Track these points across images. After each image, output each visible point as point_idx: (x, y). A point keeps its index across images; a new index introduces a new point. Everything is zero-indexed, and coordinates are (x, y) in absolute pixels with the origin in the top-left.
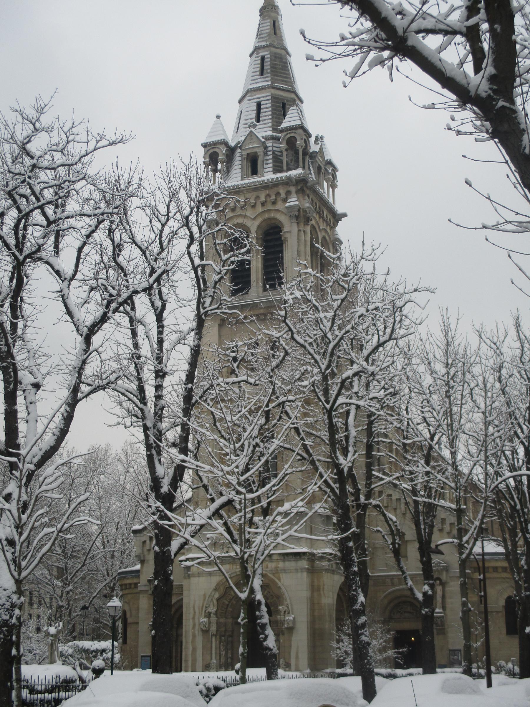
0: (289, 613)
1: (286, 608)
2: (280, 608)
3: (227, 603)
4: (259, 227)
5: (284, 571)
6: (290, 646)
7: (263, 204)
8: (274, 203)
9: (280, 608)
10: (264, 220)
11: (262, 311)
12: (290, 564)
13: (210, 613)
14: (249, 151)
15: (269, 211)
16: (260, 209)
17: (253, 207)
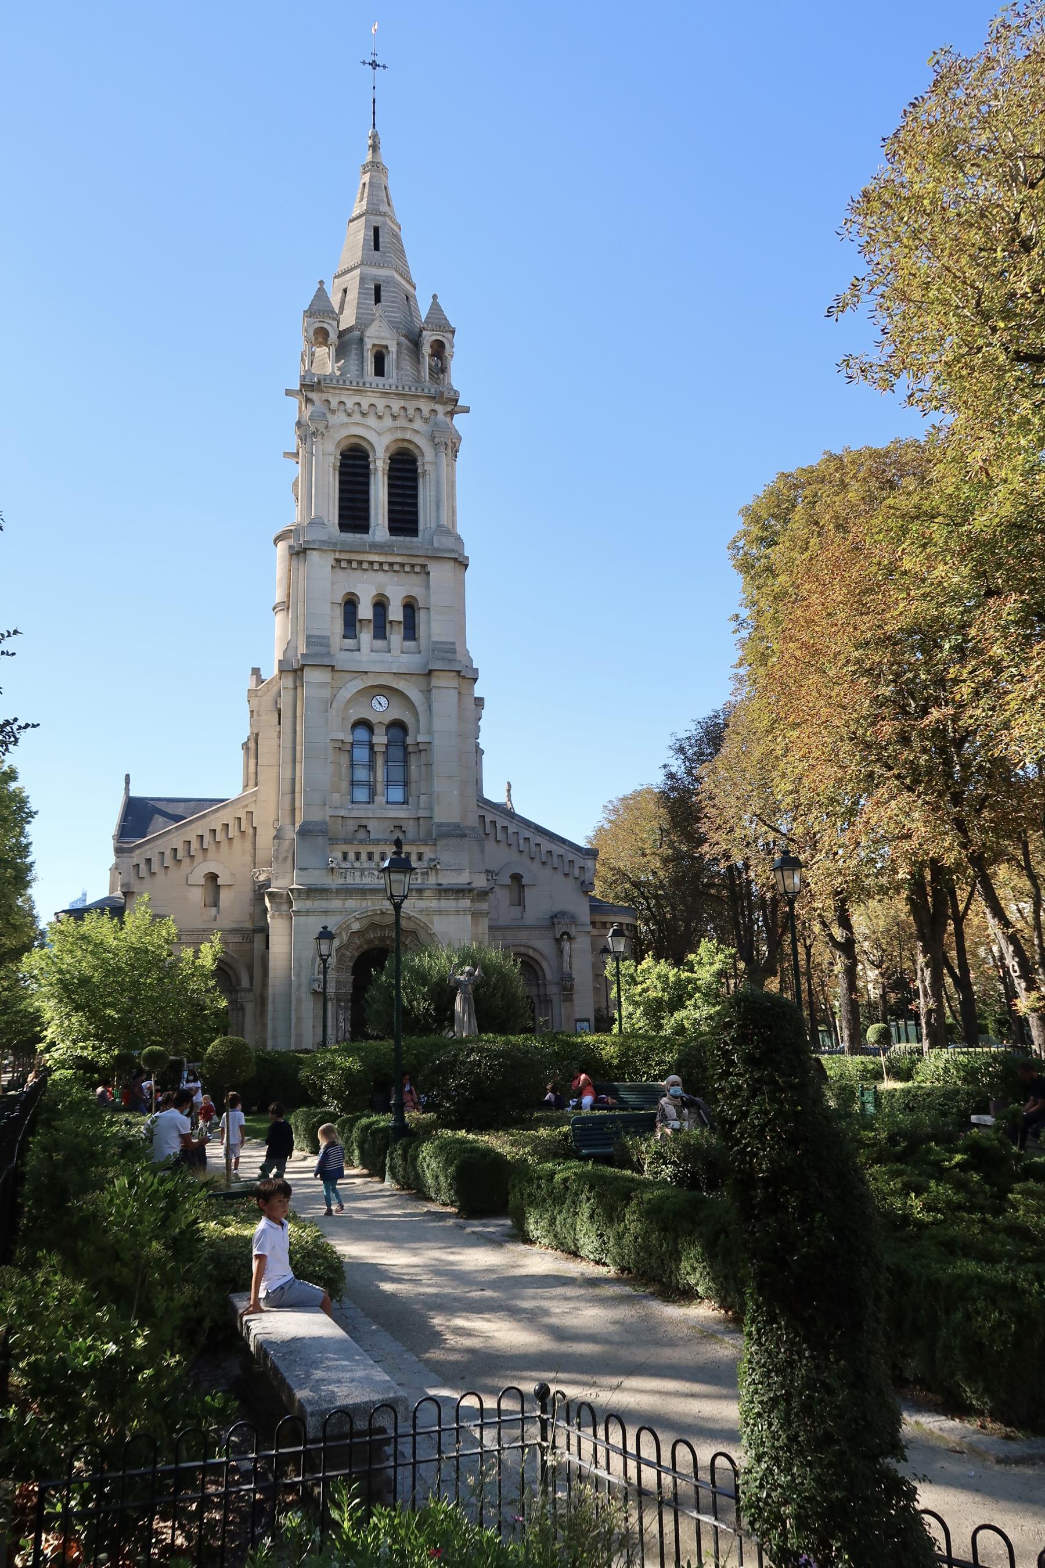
4: (387, 448)
5: (440, 912)
7: (394, 417)
10: (397, 440)
11: (398, 559)
14: (376, 342)
15: (403, 429)
17: (380, 417)
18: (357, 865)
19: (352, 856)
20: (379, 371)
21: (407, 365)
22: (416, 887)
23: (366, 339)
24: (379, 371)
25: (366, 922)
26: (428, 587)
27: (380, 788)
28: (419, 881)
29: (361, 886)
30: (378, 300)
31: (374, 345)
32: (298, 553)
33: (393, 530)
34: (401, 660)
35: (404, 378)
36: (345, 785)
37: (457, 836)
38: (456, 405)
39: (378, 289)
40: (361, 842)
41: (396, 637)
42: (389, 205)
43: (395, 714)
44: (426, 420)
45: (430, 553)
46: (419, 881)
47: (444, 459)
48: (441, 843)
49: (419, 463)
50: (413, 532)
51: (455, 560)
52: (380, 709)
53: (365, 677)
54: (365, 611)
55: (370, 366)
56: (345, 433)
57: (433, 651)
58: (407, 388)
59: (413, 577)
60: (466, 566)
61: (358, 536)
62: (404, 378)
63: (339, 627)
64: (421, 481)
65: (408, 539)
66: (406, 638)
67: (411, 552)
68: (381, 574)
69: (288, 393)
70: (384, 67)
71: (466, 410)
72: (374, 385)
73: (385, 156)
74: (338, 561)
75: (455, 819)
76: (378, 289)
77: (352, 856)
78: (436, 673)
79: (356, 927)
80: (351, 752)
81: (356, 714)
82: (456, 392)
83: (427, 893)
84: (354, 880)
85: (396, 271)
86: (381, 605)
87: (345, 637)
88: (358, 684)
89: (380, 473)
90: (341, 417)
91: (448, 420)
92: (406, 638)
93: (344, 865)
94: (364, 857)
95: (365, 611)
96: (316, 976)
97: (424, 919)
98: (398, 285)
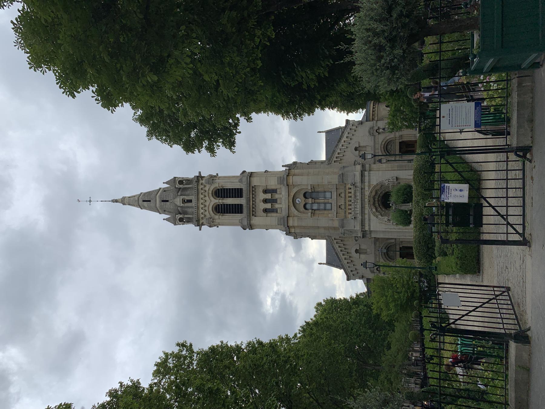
0: (389, 179)
1: (387, 181)
2: (386, 184)
3: (383, 212)
5: (369, 182)
6: (405, 179)
7: (205, 196)
8: (206, 191)
9: (386, 184)
10: (212, 196)
11: (251, 195)
12: (367, 179)
13: (388, 220)
16: (207, 198)
18: (353, 210)
19: (350, 211)
20: (190, 201)
21: (188, 192)
22: (360, 190)
23: (181, 205)
24: (190, 201)
25: (372, 207)
26: (260, 186)
27: (326, 201)
28: (358, 189)
29: (360, 208)
30: (167, 201)
31: (183, 203)
32: (251, 227)
33: (241, 197)
34: (284, 194)
35: (192, 193)
36: (326, 212)
37: (343, 176)
38: (199, 176)
39: (163, 201)
40: (345, 208)
41: (276, 196)
42: (134, 197)
43: (302, 196)
44: (205, 186)
45: (248, 185)
46: (358, 189)
47: (217, 181)
48: (345, 182)
49: (219, 188)
50: (241, 189)
51: (250, 177)
52: (300, 200)
53: (290, 206)
54: (268, 206)
55: (189, 204)
56: (211, 212)
57: (281, 184)
58: (195, 193)
59: (256, 191)
60: (252, 173)
61: (244, 208)
62: (192, 193)
63: (274, 214)
64: (224, 188)
65: (244, 192)
66: (276, 192)
67: (249, 192)
68: (256, 201)
69: (200, 229)
70: (90, 198)
71: (200, 173)
72: (196, 203)
73: (119, 197)
74: (253, 215)
75: (336, 177)
76: (163, 201)
77: (350, 211)
78: (288, 183)
79: (374, 210)
80: (315, 210)
81: (302, 209)
82: (195, 177)
83: (363, 187)
84: (358, 210)
85: (156, 195)
86: (265, 201)
87: (277, 212)
88: (292, 208)
89: (224, 201)
90: (207, 213)
91: (204, 179)
92: (276, 192)
93: (353, 214)
94: (350, 207)
95: (268, 206)
96: (391, 223)
97: (372, 187)
98: (161, 194)
